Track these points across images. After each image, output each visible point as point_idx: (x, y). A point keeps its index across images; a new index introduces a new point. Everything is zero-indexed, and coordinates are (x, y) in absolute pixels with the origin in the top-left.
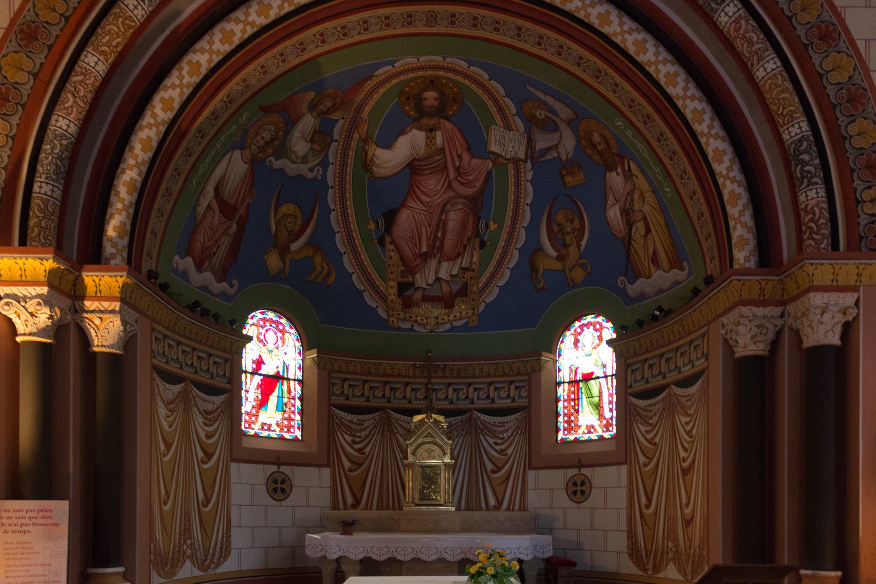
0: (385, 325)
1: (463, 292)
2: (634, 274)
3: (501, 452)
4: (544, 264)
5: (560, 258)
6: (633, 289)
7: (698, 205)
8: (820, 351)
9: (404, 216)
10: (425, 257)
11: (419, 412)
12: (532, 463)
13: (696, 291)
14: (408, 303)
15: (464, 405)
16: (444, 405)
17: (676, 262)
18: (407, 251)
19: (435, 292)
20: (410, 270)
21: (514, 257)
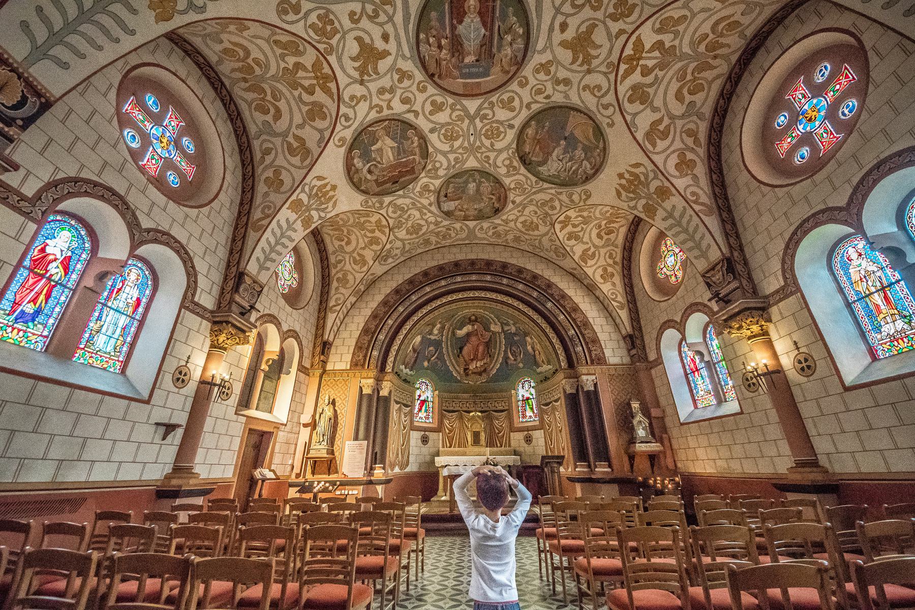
0: (459, 382)
1: (485, 370)
2: (538, 366)
3: (501, 426)
4: (510, 362)
5: (515, 360)
6: (539, 370)
7: (550, 348)
8: (588, 393)
9: (465, 348)
10: (472, 360)
11: (472, 412)
12: (512, 429)
13: (554, 373)
14: (467, 375)
15: (488, 409)
16: (480, 409)
17: (549, 363)
18: (467, 359)
19: (475, 371)
20: (467, 364)
21: (501, 360)
